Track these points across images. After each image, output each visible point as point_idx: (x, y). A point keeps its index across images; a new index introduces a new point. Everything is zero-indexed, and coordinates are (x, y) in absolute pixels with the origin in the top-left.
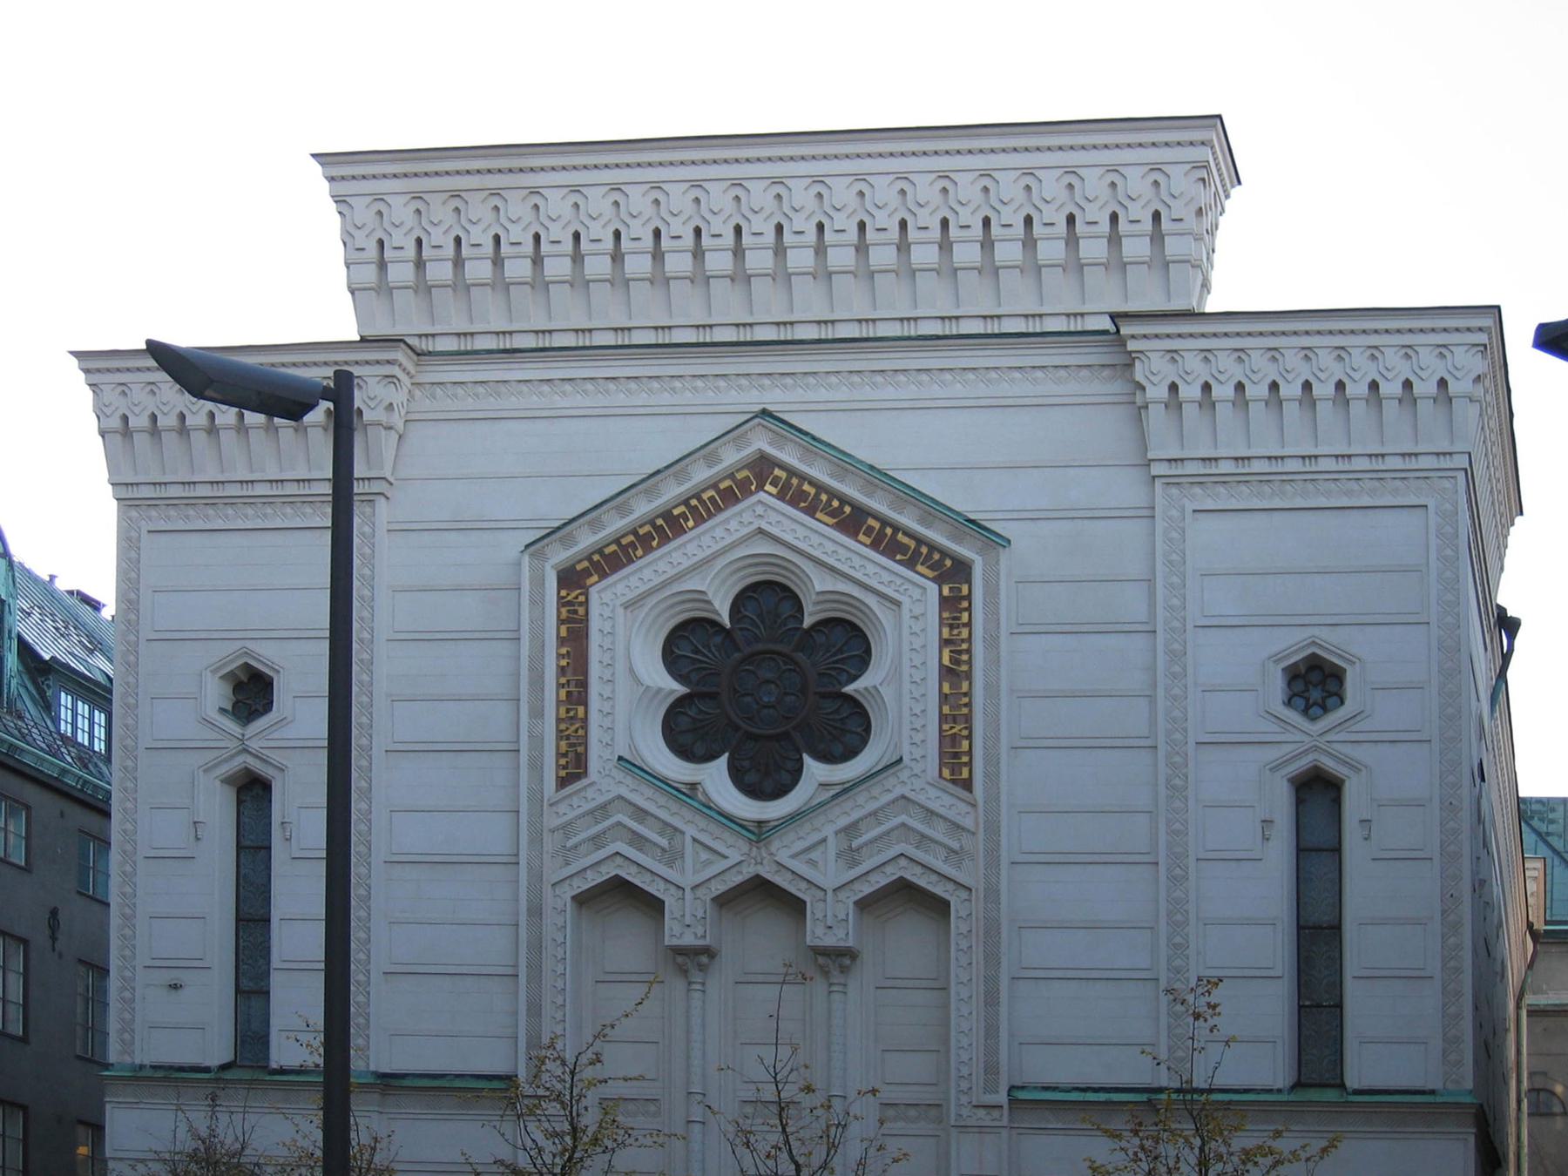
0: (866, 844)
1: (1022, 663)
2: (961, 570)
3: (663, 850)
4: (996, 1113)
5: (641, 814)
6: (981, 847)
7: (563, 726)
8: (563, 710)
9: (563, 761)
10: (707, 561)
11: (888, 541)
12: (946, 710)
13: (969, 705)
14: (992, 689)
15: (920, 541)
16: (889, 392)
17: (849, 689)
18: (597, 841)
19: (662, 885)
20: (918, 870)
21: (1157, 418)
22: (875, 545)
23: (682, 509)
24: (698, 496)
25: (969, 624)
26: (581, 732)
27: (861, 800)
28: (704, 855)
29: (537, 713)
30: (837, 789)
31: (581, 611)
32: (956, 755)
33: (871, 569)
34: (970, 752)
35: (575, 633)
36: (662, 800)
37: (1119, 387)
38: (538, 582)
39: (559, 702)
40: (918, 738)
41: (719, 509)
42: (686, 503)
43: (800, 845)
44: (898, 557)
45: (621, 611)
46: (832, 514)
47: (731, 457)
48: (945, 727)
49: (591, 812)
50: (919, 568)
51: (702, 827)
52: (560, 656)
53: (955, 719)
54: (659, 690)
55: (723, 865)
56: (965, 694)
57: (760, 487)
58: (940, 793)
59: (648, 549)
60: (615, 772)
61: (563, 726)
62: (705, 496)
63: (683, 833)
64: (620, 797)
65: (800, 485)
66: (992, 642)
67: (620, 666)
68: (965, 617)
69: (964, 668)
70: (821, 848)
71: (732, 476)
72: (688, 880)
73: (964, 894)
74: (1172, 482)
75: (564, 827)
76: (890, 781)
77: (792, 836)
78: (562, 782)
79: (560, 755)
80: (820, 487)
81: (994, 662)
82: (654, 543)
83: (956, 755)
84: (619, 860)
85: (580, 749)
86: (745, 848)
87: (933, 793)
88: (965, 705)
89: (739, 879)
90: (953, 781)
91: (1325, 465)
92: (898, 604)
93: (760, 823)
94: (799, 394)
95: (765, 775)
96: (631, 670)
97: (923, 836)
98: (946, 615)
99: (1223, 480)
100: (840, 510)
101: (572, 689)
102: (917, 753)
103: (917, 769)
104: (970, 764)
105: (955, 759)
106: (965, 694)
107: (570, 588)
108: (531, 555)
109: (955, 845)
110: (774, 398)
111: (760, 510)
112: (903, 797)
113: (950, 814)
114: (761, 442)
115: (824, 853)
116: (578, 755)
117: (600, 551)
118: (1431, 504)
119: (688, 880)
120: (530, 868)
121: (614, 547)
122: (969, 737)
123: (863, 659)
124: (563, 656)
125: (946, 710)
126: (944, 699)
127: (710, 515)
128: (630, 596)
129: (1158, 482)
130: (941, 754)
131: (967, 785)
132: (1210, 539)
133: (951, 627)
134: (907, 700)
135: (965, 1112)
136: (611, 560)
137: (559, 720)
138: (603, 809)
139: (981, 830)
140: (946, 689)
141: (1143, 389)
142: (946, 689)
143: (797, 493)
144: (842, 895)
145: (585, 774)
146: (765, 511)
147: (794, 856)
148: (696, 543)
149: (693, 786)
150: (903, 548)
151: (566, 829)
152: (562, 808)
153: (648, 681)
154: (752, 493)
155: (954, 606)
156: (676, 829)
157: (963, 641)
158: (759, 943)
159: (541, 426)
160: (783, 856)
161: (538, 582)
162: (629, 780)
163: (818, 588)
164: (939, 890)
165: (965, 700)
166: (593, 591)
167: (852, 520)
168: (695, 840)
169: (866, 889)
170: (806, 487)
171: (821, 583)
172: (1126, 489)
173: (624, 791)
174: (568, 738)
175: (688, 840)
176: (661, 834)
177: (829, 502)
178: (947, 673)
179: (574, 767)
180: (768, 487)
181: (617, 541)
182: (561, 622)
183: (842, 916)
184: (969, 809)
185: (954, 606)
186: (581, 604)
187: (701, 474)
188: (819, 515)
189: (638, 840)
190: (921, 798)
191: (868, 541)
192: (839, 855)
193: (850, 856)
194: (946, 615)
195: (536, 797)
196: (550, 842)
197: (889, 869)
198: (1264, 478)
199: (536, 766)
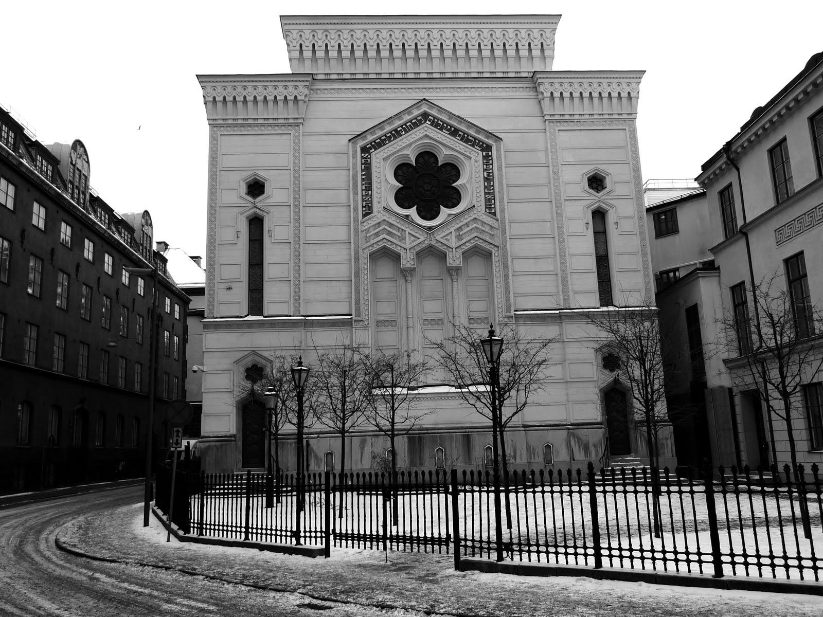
1: (508, 177)
4: (511, 319)
5: (391, 225)
10: (410, 145)
11: (466, 139)
12: (486, 191)
13: (493, 189)
14: (501, 183)
15: (476, 139)
16: (463, 94)
18: (377, 235)
19: (399, 248)
20: (481, 241)
21: (546, 103)
22: (461, 140)
24: (405, 124)
25: (492, 164)
28: (412, 238)
29: (356, 193)
31: (369, 160)
32: (490, 205)
33: (462, 147)
34: (494, 204)
35: (367, 168)
36: (398, 221)
37: (532, 94)
39: (362, 190)
40: (479, 200)
41: (412, 129)
42: (402, 126)
43: (444, 234)
46: (447, 130)
47: (416, 113)
49: (375, 225)
51: (410, 231)
52: (362, 175)
53: (489, 193)
55: (419, 241)
57: (425, 122)
59: (390, 141)
63: (405, 231)
66: (500, 169)
67: (382, 179)
71: (416, 119)
72: (408, 246)
73: (496, 249)
74: (551, 121)
78: (364, 216)
79: (363, 207)
80: (444, 123)
81: (501, 175)
83: (490, 205)
84: (385, 241)
87: (484, 217)
89: (424, 245)
91: (596, 117)
92: (470, 158)
93: (430, 228)
95: (429, 212)
96: (386, 180)
99: (566, 121)
100: (450, 129)
104: (495, 207)
105: (490, 206)
107: (365, 154)
109: (492, 233)
110: (427, 95)
111: (426, 129)
114: (425, 108)
115: (451, 237)
117: (374, 142)
118: (627, 128)
119: (408, 246)
120: (355, 244)
122: (494, 199)
123: (458, 176)
125: (486, 191)
126: (485, 187)
127: (410, 131)
128: (386, 155)
129: (547, 122)
130: (486, 204)
131: (494, 214)
132: (564, 138)
134: (474, 188)
135: (501, 319)
136: (378, 144)
137: (363, 196)
138: (379, 224)
140: (486, 184)
141: (542, 93)
144: (458, 250)
146: (426, 129)
149: (407, 216)
150: (471, 141)
151: (367, 231)
152: (365, 224)
155: (487, 158)
158: (430, 267)
159: (353, 103)
160: (438, 238)
161: (355, 152)
162: (387, 214)
164: (489, 247)
167: (454, 132)
169: (465, 248)
171: (446, 152)
172: (537, 123)
178: (486, 179)
179: (368, 210)
181: (380, 138)
182: (362, 164)
183: (458, 256)
185: (487, 158)
187: (407, 118)
189: (390, 233)
193: (460, 237)
195: (356, 220)
196: (362, 235)
197: (472, 241)
198: (579, 121)
199: (356, 210)
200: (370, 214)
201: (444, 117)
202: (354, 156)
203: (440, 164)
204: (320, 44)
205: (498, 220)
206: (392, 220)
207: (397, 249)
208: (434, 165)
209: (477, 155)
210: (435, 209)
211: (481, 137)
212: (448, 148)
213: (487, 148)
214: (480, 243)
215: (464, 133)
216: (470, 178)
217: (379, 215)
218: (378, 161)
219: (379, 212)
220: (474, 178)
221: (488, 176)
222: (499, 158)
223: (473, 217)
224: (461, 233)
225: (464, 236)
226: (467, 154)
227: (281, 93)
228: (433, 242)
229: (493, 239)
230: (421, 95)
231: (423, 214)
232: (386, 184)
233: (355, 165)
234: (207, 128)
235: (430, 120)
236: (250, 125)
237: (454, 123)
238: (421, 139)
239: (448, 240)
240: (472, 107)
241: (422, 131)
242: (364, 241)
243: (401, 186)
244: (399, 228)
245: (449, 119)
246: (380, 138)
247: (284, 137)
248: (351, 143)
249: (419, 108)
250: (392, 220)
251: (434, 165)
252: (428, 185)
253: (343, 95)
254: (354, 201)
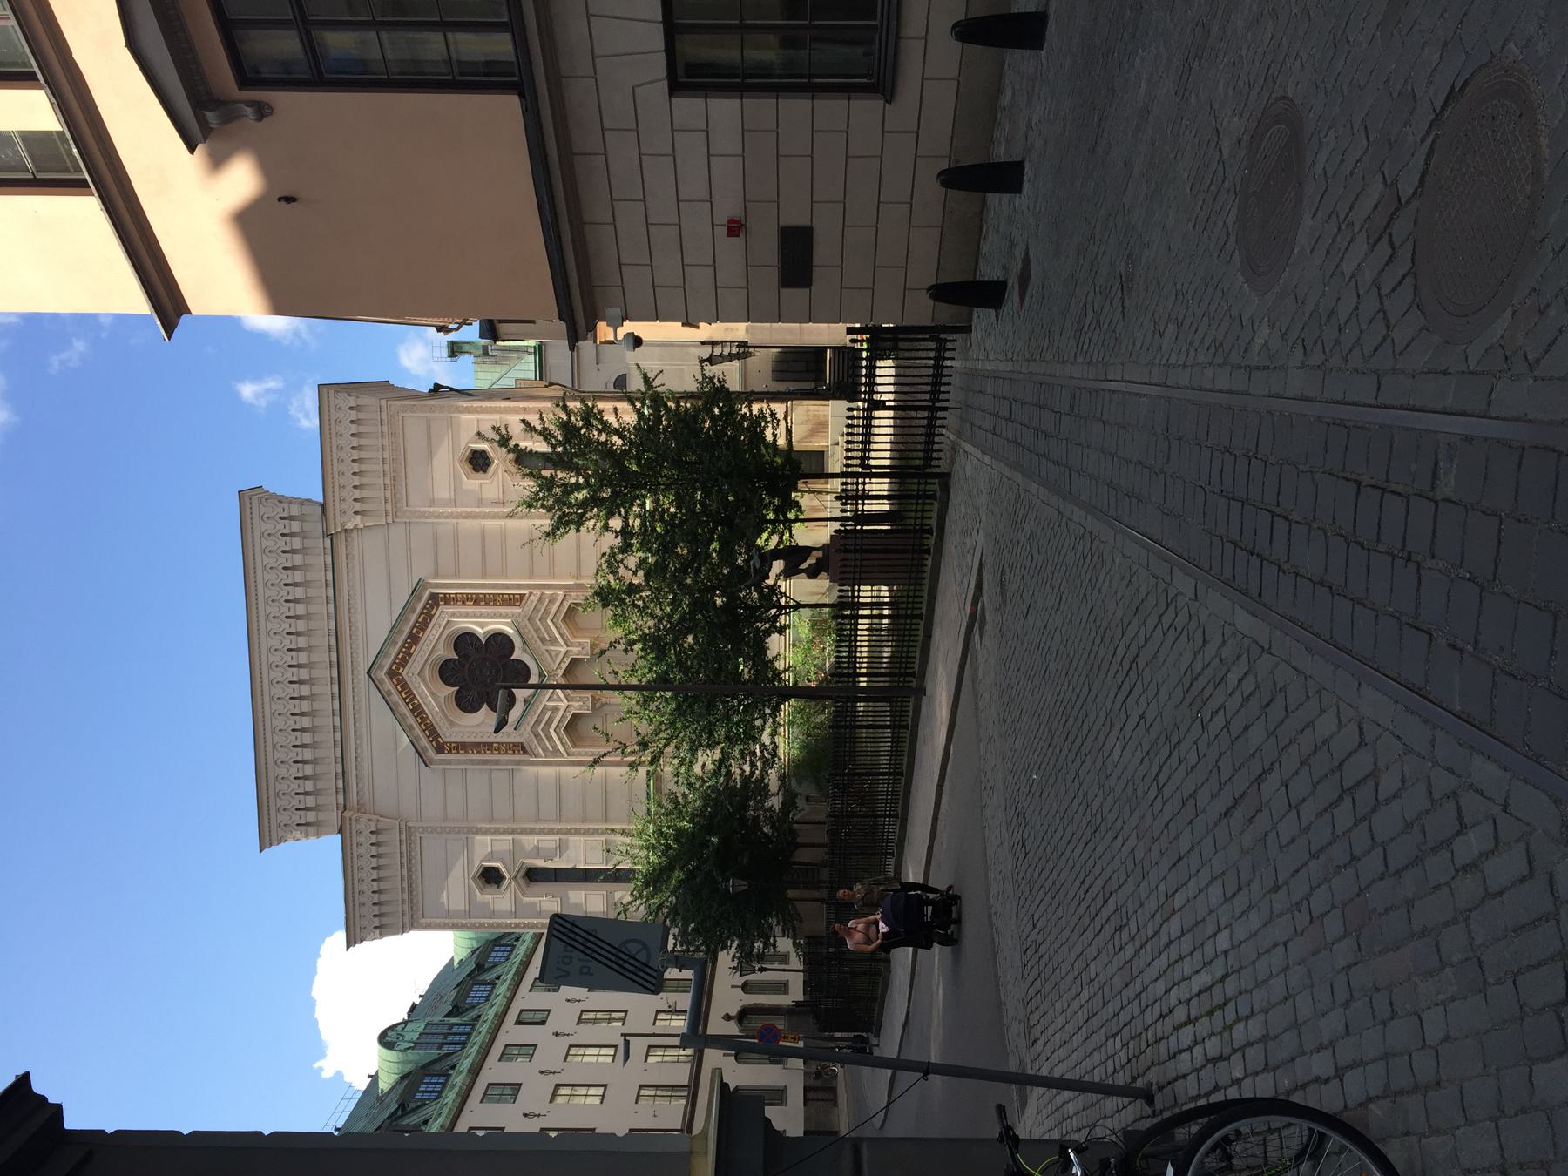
2: (434, 596)
5: (538, 721)
10: (432, 694)
11: (423, 625)
29: (497, 762)
38: (442, 762)
47: (388, 685)
78: (525, 752)
94: (361, 660)
105: (511, 601)
114: (382, 674)
131: (522, 596)
138: (537, 736)
146: (410, 673)
155: (448, 600)
161: (442, 762)
167: (414, 639)
172: (397, 533)
185: (448, 600)
189: (549, 723)
193: (554, 641)
201: (394, 651)
202: (449, 762)
204: (296, 802)
207: (569, 716)
209: (445, 611)
212: (435, 645)
213: (435, 600)
227: (367, 850)
230: (363, 676)
233: (459, 762)
234: (414, 936)
236: (410, 885)
240: (375, 619)
247: (424, 844)
249: (382, 682)
252: (485, 672)
253: (365, 772)
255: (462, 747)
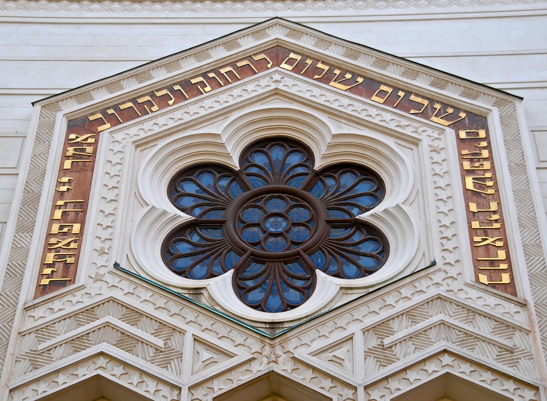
0: (401, 341)
2: (478, 120)
3: (157, 349)
5: (134, 315)
6: (540, 346)
7: (53, 240)
8: (55, 229)
9: (48, 271)
11: (401, 99)
13: (500, 220)
15: (432, 101)
17: (365, 216)
18: (77, 343)
23: (201, 79)
25: (490, 158)
26: (73, 245)
27: (390, 300)
28: (206, 355)
29: (25, 227)
30: (365, 292)
31: (89, 150)
33: (388, 116)
36: (161, 302)
38: (46, 127)
39: (52, 220)
40: (449, 245)
42: (204, 75)
44: (412, 111)
45: (130, 148)
48: (476, 239)
50: (434, 119)
52: (60, 184)
53: (485, 232)
54: (165, 213)
56: (495, 212)
58: (481, 294)
60: (108, 278)
61: (53, 240)
62: (223, 71)
63: (182, 332)
64: (112, 300)
65: (313, 66)
66: (518, 168)
68: (485, 154)
69: (490, 191)
70: (345, 348)
72: (186, 380)
75: (37, 330)
76: (422, 285)
77: (313, 334)
78: (42, 290)
79: (44, 265)
82: (171, 102)
84: (102, 361)
85: (69, 260)
86: (256, 347)
87: (474, 293)
88: (496, 221)
89: (247, 378)
90: (493, 286)
92: (415, 142)
93: (273, 325)
97: (467, 334)
98: (465, 152)
101: (69, 209)
102: (451, 258)
103: (452, 272)
104: (510, 270)
105: (492, 267)
106: (495, 212)
107: (79, 133)
108: (43, 107)
111: (277, 77)
112: (439, 297)
113: (498, 312)
114: (277, 34)
115: (351, 352)
116: (67, 265)
117: (116, 107)
119: (186, 380)
121: (130, 104)
122: (506, 247)
123: (379, 192)
124: (64, 184)
125: (476, 225)
126: (471, 216)
127: (227, 82)
130: (476, 262)
133: (471, 160)
137: (50, 235)
138: (90, 312)
139: (537, 330)
140: (473, 207)
142: (473, 207)
143: (308, 67)
145: (73, 281)
147: (317, 353)
148: (214, 99)
149: (197, 291)
150: (418, 106)
151: (44, 331)
152: (39, 312)
153: (152, 201)
154: (268, 68)
156: (174, 329)
157: (486, 171)
160: (302, 354)
161: (46, 127)
163: (334, 131)
165: (495, 217)
166: (105, 139)
168: (196, 339)
170: (320, 65)
173: (118, 295)
174: (57, 250)
175: (189, 340)
176: (156, 334)
177: (342, 75)
179: (60, 275)
180: (283, 65)
182: (65, 157)
184: (518, 309)
186: (90, 144)
187: (219, 54)
188: (332, 83)
189: (127, 341)
190: (461, 297)
191: (382, 101)
192: (368, 353)
193: (382, 354)
194: (465, 152)
197: (431, 367)
200: (63, 284)
201: (334, 53)
203: (319, 164)
205: (523, 305)
206: (142, 300)
208: (300, 170)
210: (299, 284)
211: (452, 93)
213: (470, 126)
214: (462, 371)
215: (396, 89)
216: (417, 194)
217: (94, 288)
218: (117, 147)
219: (98, 278)
220: (430, 187)
221: (480, 182)
222: (513, 141)
223: (432, 292)
224: (387, 341)
225: (397, 350)
226: (408, 131)
228: (284, 368)
229: (514, 363)
231: (256, 296)
232: (134, 203)
235: (290, 62)
237: (364, 63)
238: (260, 99)
239: (337, 361)
241: (263, 82)
242: (25, 364)
243: (185, 217)
244: (162, 324)
245: (346, 55)
246: (134, 101)
248: (38, 107)
250: (142, 300)
251: (300, 170)
254: (15, 247)
255: (81, 163)
